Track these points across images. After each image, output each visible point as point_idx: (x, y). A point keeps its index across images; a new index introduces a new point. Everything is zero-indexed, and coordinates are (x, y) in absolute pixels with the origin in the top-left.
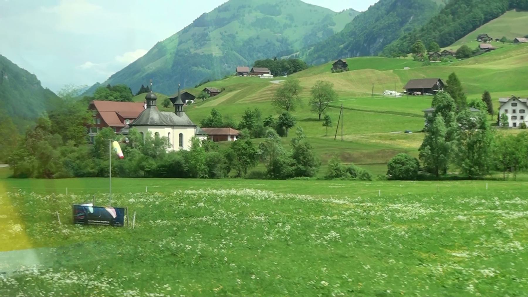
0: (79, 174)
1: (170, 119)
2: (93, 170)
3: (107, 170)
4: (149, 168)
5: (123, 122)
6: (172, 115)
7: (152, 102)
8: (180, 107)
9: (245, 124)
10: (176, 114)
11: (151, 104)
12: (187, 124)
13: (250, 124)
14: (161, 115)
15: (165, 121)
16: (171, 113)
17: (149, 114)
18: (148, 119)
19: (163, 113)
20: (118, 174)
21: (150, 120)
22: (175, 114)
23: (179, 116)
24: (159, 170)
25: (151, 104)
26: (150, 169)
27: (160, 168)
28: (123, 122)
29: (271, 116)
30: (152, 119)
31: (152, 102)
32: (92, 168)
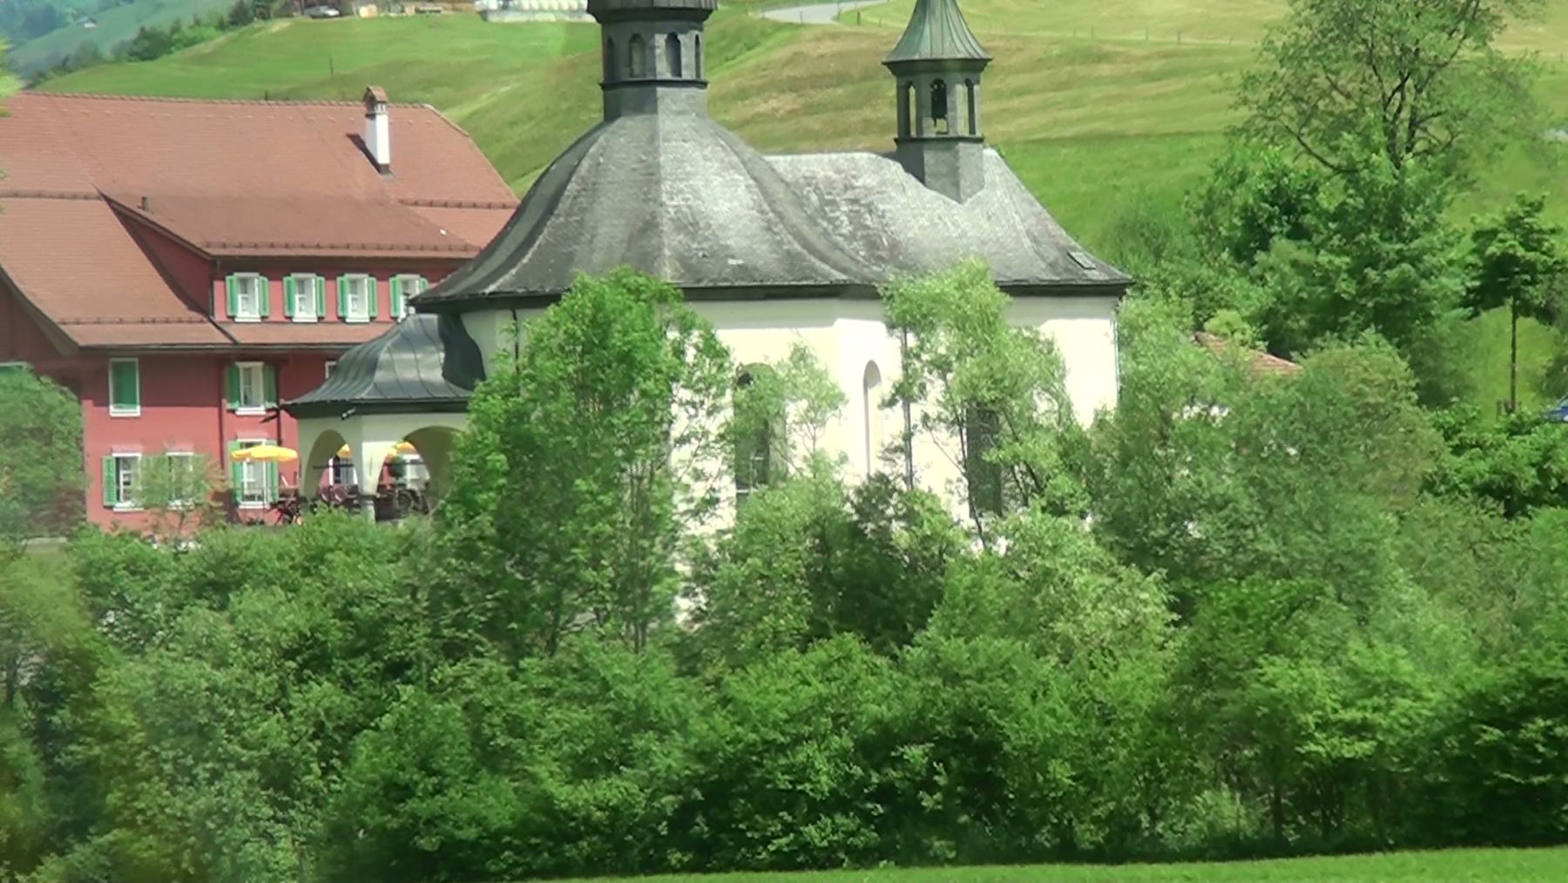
0: (427, 843)
1: (855, 218)
2: (610, 790)
3: (783, 782)
4: (1357, 730)
5: (201, 304)
6: (867, 180)
7: (674, 42)
8: (960, 90)
9: (1346, 287)
10: (917, 170)
11: (663, 70)
12: (1047, 276)
13: (1405, 286)
14: (767, 178)
15: (820, 244)
16: (862, 158)
17: (651, 175)
18: (649, 226)
19: (781, 162)
20: (940, 822)
21: (672, 241)
22: (895, 168)
23: (952, 186)
24: (1497, 753)
25: (663, 70)
26: (1365, 747)
27: (1511, 720)
28: (201, 304)
29: (1537, 207)
30: (690, 225)
31: (674, 42)
32: (583, 769)
